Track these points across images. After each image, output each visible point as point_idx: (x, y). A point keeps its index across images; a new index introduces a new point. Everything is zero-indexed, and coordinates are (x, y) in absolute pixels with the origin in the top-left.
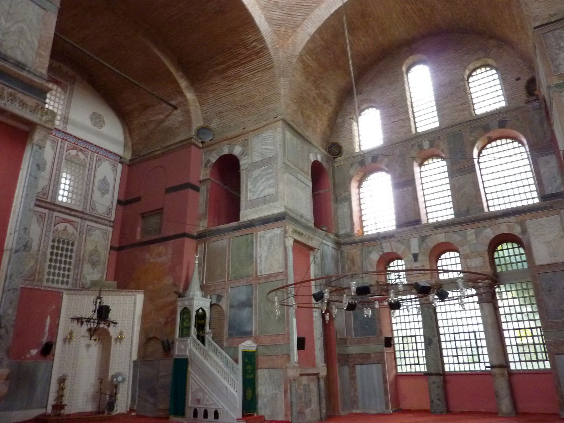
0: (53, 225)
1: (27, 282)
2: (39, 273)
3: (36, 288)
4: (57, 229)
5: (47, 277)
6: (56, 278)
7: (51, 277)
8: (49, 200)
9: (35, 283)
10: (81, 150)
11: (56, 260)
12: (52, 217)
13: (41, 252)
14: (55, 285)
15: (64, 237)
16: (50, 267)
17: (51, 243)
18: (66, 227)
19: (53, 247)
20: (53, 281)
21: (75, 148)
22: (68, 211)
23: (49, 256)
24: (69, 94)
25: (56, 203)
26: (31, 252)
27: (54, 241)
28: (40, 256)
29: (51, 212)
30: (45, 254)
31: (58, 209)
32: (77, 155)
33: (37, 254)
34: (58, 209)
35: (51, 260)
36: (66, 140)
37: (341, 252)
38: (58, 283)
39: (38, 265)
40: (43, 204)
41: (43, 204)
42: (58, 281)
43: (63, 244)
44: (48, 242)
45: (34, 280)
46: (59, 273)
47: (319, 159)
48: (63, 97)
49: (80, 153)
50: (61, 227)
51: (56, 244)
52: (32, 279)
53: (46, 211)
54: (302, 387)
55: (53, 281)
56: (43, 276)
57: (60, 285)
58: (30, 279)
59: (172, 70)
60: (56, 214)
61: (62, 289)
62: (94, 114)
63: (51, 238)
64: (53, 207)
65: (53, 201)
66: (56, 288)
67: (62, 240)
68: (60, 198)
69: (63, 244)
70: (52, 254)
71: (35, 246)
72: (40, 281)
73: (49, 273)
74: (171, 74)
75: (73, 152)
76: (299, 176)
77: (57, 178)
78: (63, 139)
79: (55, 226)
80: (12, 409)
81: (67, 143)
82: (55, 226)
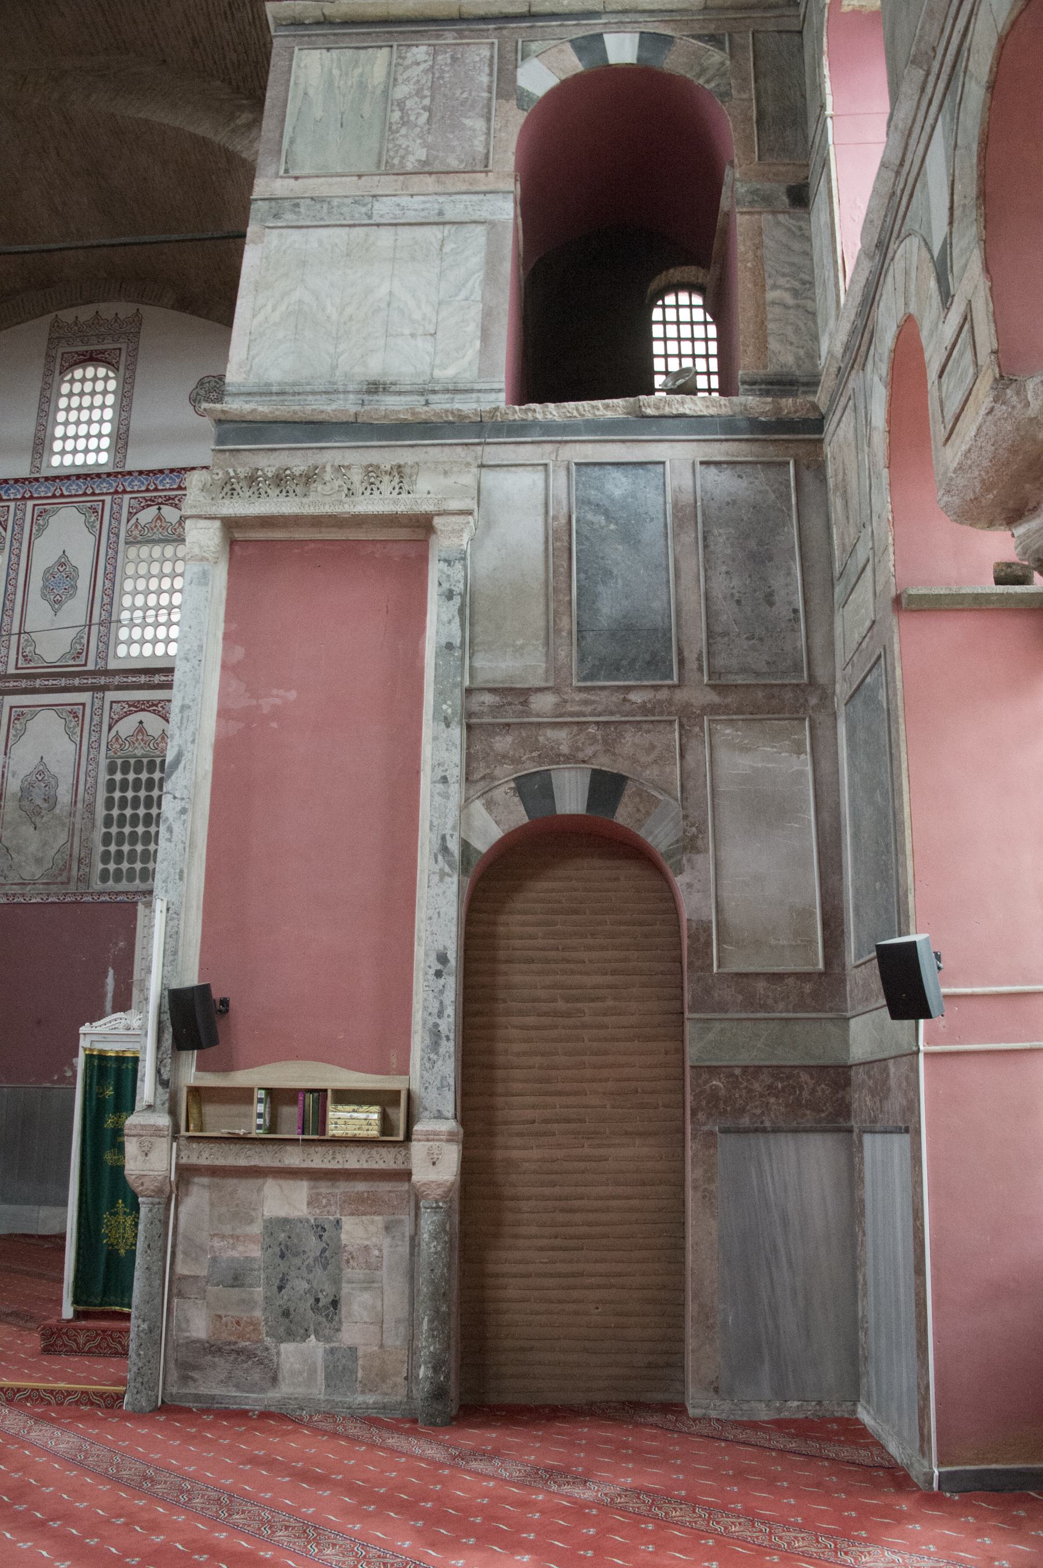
0: (105, 727)
1: (54, 888)
2: (79, 861)
3: (68, 899)
4: (117, 736)
5: (101, 866)
6: (125, 866)
7: (112, 866)
8: (90, 667)
9: (72, 888)
10: (170, 498)
11: (122, 819)
12: (102, 708)
13: (80, 805)
14: (124, 885)
15: (139, 752)
16: (107, 839)
17: (103, 777)
18: (141, 722)
19: (111, 786)
20: (118, 875)
21: (150, 502)
22: (143, 679)
23: (101, 812)
24: (127, 368)
25: (112, 665)
26: (57, 811)
27: (112, 769)
28: (78, 818)
29: (100, 695)
30: (90, 808)
31: (117, 680)
32: (159, 518)
33: (72, 814)
34: (117, 680)
35: (108, 821)
36: (124, 492)
37: (815, 466)
38: (131, 878)
39: (76, 839)
40: (77, 682)
41: (77, 682)
42: (118, 873)
43: (138, 770)
44: (96, 778)
45: (68, 883)
46: (133, 852)
47: (622, 49)
48: (112, 385)
49: (166, 510)
50: (127, 727)
51: (118, 776)
52: (63, 878)
53: (85, 697)
54: (256, 1229)
55: (118, 875)
56: (90, 865)
57: (124, 885)
58: (59, 879)
59: (203, 129)
60: (111, 695)
61: (136, 893)
62: (201, 383)
63: (103, 763)
64: (103, 680)
65: (101, 664)
66: (118, 894)
67: (132, 761)
68: (122, 651)
69: (138, 770)
70: (109, 803)
71: (64, 794)
72: (84, 879)
73: (106, 857)
74: (204, 142)
75: (147, 515)
76: (383, 209)
77: (107, 600)
78: (116, 492)
79: (110, 728)
80: (40, 1203)
81: (127, 497)
82: (110, 728)
